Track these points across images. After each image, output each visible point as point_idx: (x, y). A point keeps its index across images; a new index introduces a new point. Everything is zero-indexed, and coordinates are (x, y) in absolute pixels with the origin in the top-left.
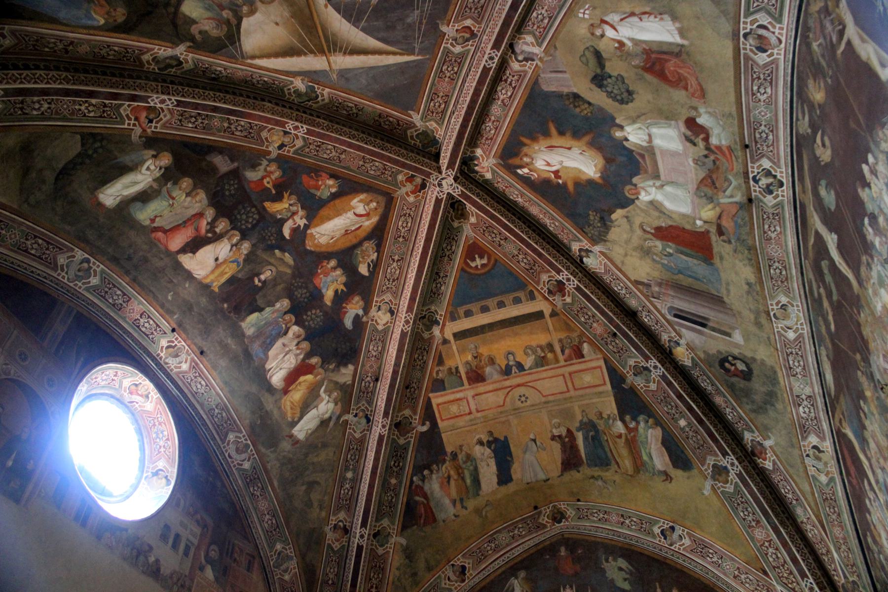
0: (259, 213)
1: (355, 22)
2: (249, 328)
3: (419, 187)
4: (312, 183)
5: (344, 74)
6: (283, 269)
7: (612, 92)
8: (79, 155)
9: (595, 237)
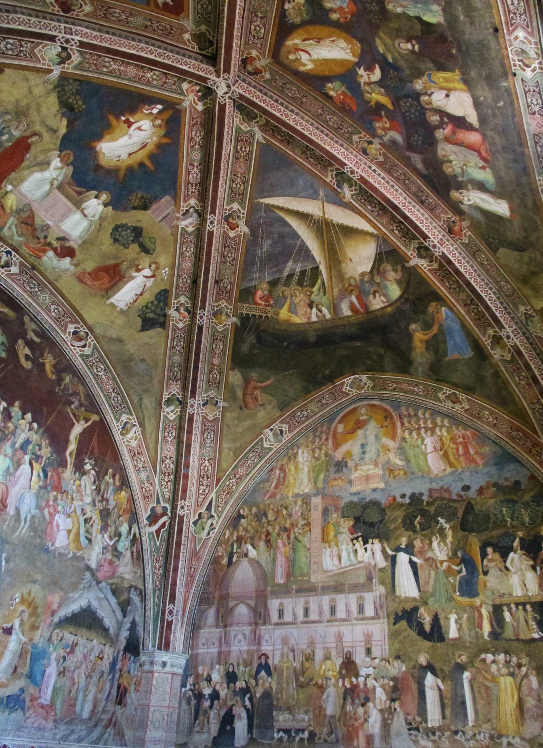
0: (399, 105)
1: (303, 244)
2: (437, 12)
3: (248, 62)
4: (349, 101)
5: (314, 196)
6: (388, 41)
7: (126, 231)
8: (504, 247)
9: (66, 83)
